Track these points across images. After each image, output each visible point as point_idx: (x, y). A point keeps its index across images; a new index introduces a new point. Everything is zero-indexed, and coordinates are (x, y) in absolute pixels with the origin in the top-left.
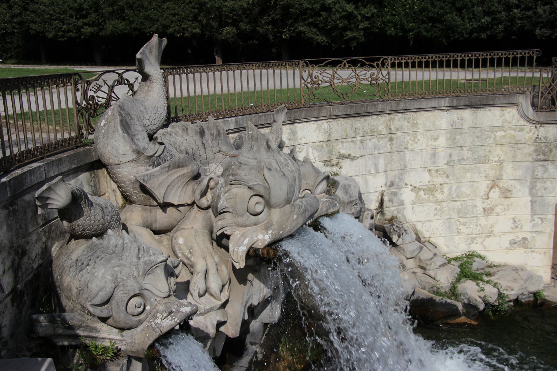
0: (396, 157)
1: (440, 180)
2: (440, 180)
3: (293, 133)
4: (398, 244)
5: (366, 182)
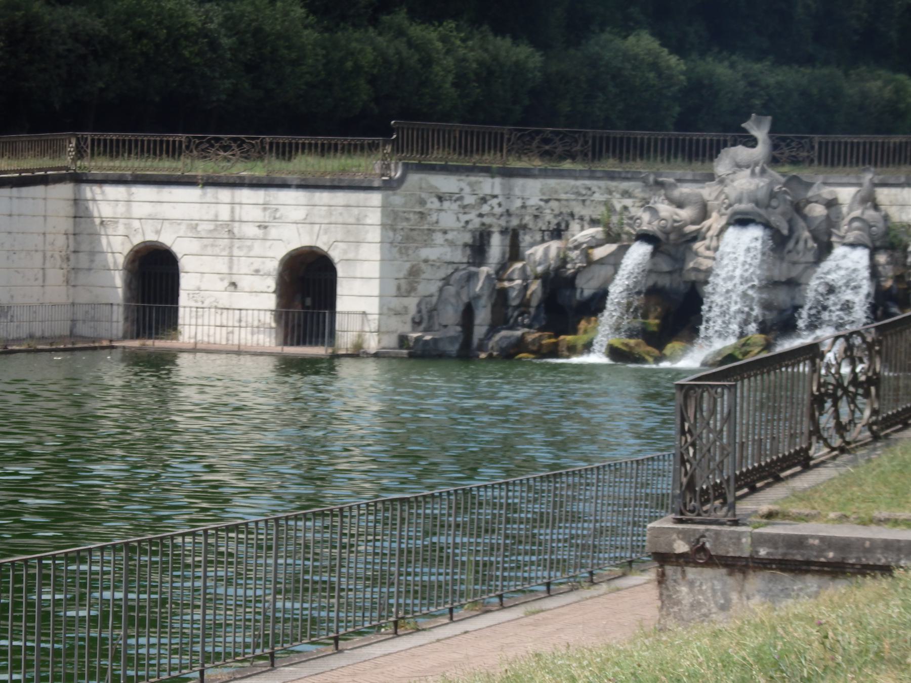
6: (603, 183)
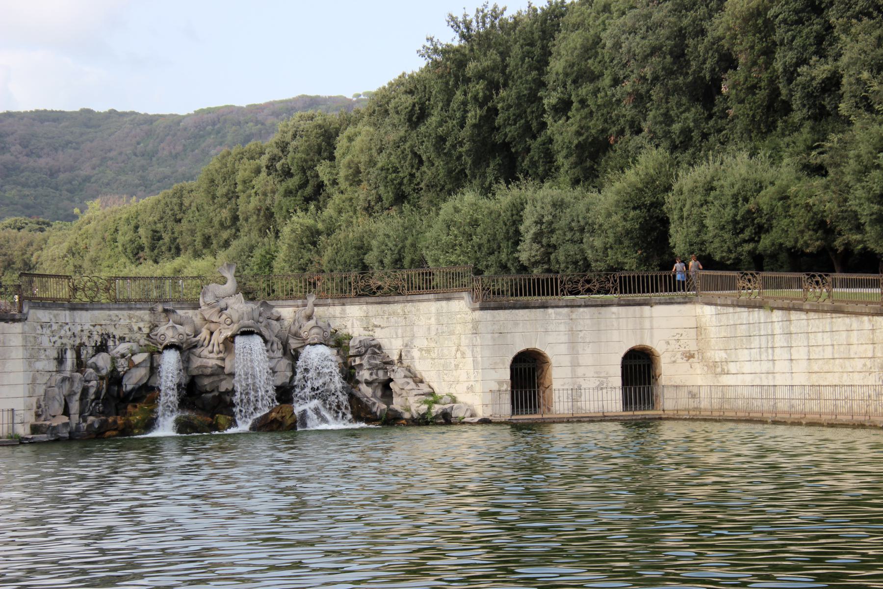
0: (408, 329)
1: (433, 345)
2: (433, 345)
3: (344, 310)
5: (391, 342)
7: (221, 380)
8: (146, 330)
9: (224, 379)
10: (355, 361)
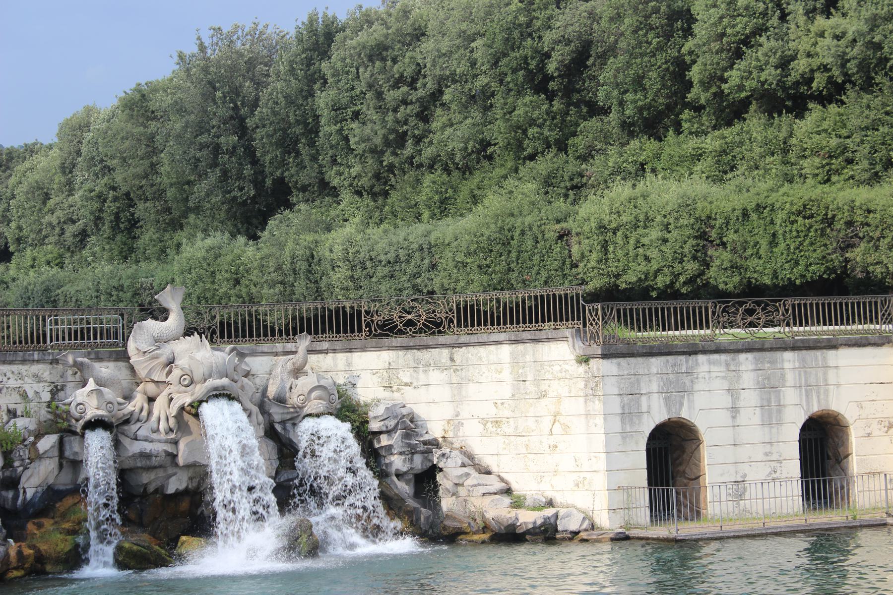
2: (507, 413)
4: (441, 465)
6: (15, 368)
7: (170, 476)
8: (46, 397)
9: (175, 474)
10: (379, 441)
